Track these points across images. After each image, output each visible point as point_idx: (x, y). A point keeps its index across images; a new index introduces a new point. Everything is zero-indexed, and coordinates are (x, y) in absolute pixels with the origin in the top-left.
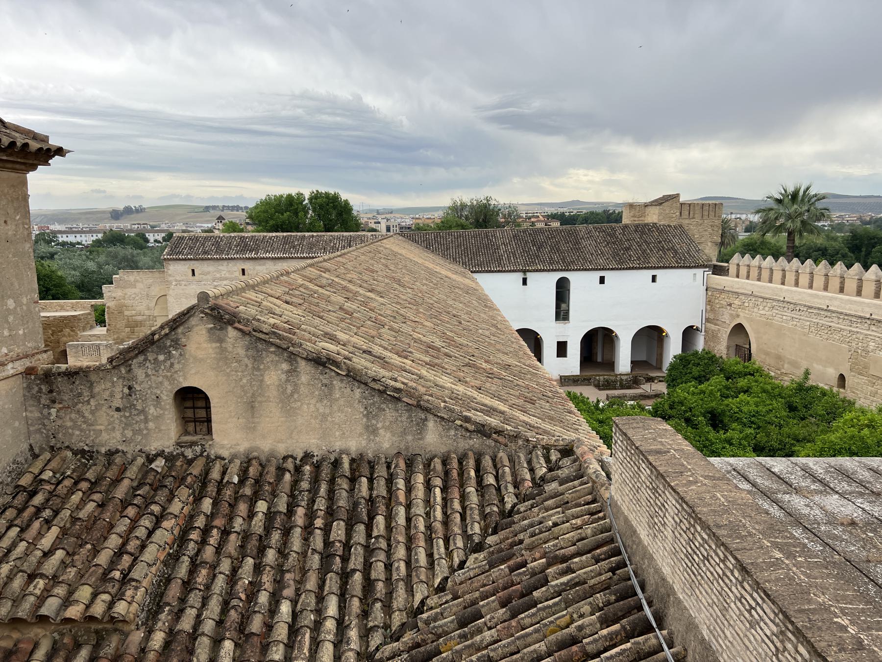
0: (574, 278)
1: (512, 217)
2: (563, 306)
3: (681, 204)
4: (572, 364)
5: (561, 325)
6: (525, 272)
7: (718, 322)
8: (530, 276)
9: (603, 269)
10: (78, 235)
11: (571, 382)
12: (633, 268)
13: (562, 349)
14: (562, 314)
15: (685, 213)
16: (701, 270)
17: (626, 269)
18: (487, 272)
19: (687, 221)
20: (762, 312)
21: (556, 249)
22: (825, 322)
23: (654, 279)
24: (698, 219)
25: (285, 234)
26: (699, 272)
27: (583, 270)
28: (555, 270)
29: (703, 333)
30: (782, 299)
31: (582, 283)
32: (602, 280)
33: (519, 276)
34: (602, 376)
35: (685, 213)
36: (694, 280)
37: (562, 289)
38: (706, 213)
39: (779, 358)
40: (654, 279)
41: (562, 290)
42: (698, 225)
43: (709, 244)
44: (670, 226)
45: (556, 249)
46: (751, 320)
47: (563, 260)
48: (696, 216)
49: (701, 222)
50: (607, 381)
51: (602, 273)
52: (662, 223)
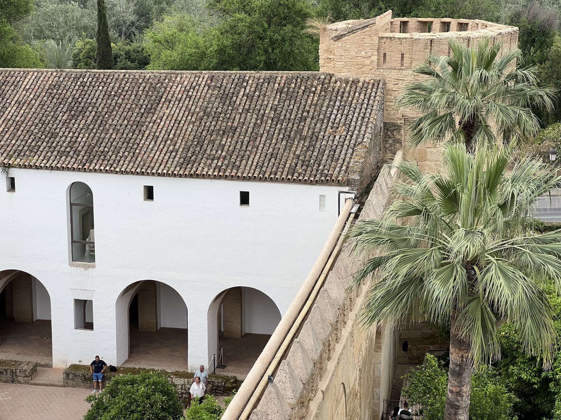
0: (102, 186)
4: (106, 342)
6: (7, 167)
11: (79, 380)
14: (82, 247)
16: (335, 190)
44: (355, 82)
51: (149, 181)
52: (343, 75)
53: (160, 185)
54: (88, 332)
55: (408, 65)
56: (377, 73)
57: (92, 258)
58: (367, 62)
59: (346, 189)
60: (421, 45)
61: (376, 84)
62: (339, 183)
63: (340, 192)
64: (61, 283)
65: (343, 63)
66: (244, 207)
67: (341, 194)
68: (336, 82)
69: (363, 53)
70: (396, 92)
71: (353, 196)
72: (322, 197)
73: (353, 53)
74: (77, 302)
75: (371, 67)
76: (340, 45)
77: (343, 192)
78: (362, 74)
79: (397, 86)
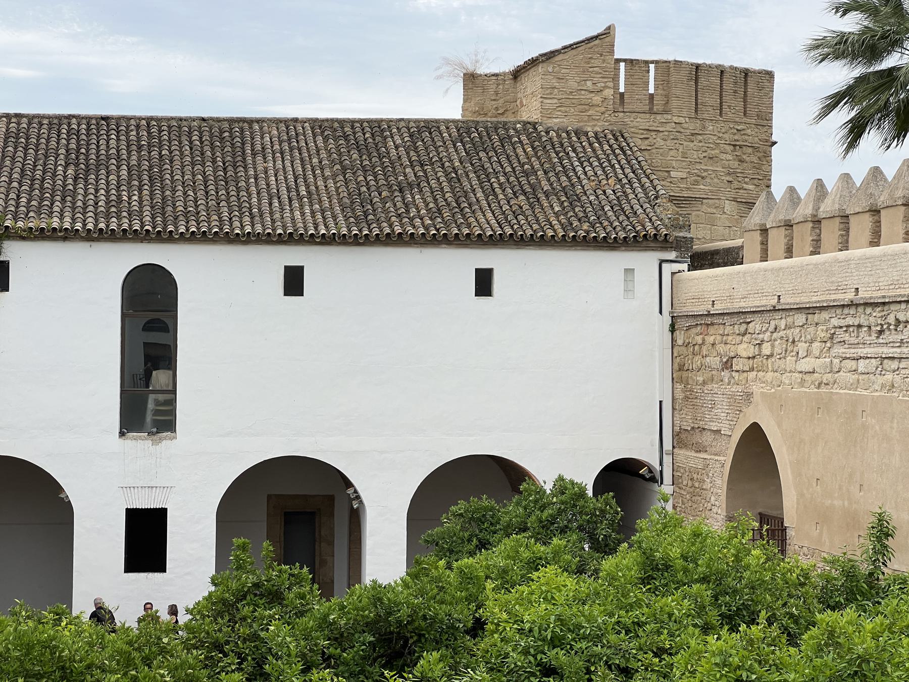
7: (707, 438)
13: (146, 538)
14: (147, 397)
19: (642, 122)
20: (806, 364)
23: (484, 283)
24: (680, 114)
26: (645, 263)
30: (850, 296)
31: (218, 289)
32: (294, 281)
36: (628, 291)
37: (150, 308)
38: (710, 99)
48: (674, 103)
49: (692, 126)
51: (294, 256)
52: (554, 122)
53: (316, 263)
54: (110, 604)
55: (661, 108)
56: (613, 119)
57: (165, 423)
58: (597, 99)
59: (672, 255)
60: (684, 72)
63: (662, 262)
65: (555, 101)
66: (483, 300)
67: (664, 265)
68: (547, 133)
69: (589, 83)
70: (645, 153)
71: (685, 266)
72: (629, 272)
73: (573, 84)
75: (603, 109)
76: (550, 70)
77: (667, 261)
78: (589, 121)
79: (647, 142)
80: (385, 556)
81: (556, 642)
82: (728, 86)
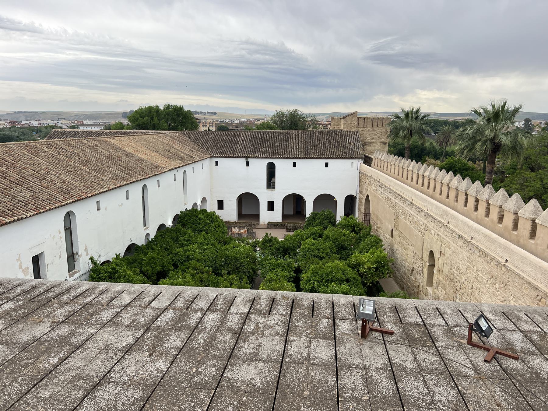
0: (277, 163)
1: (315, 122)
2: (273, 179)
3: (359, 118)
4: (277, 216)
5: (270, 191)
8: (250, 160)
9: (294, 158)
10: (93, 127)
12: (312, 158)
13: (271, 206)
14: (271, 183)
15: (361, 123)
16: (357, 160)
17: (308, 158)
18: (225, 157)
19: (362, 129)
20: (374, 188)
21: (272, 145)
22: (389, 195)
23: (327, 165)
24: (369, 128)
25: (115, 131)
26: (355, 161)
27: (281, 158)
28: (265, 158)
29: (357, 200)
31: (283, 166)
32: (295, 165)
33: (243, 161)
34: (291, 223)
35: (361, 123)
36: (352, 166)
38: (375, 124)
39: (377, 217)
40: (327, 165)
41: (271, 171)
42: (369, 131)
43: (378, 143)
44: (350, 132)
45: (272, 145)
46: (371, 193)
47: (273, 152)
50: (295, 226)
51: (295, 161)
52: (345, 130)
53: (298, 161)
57: (274, 188)
61: (357, 132)
62: (359, 158)
64: (264, 196)
74: (268, 202)
80: (309, 210)
81: (308, 251)
82: (379, 121)
